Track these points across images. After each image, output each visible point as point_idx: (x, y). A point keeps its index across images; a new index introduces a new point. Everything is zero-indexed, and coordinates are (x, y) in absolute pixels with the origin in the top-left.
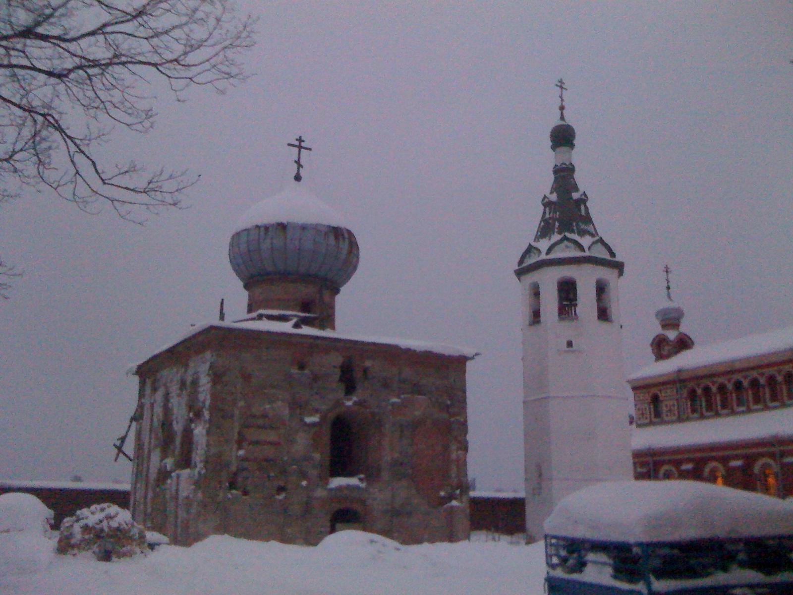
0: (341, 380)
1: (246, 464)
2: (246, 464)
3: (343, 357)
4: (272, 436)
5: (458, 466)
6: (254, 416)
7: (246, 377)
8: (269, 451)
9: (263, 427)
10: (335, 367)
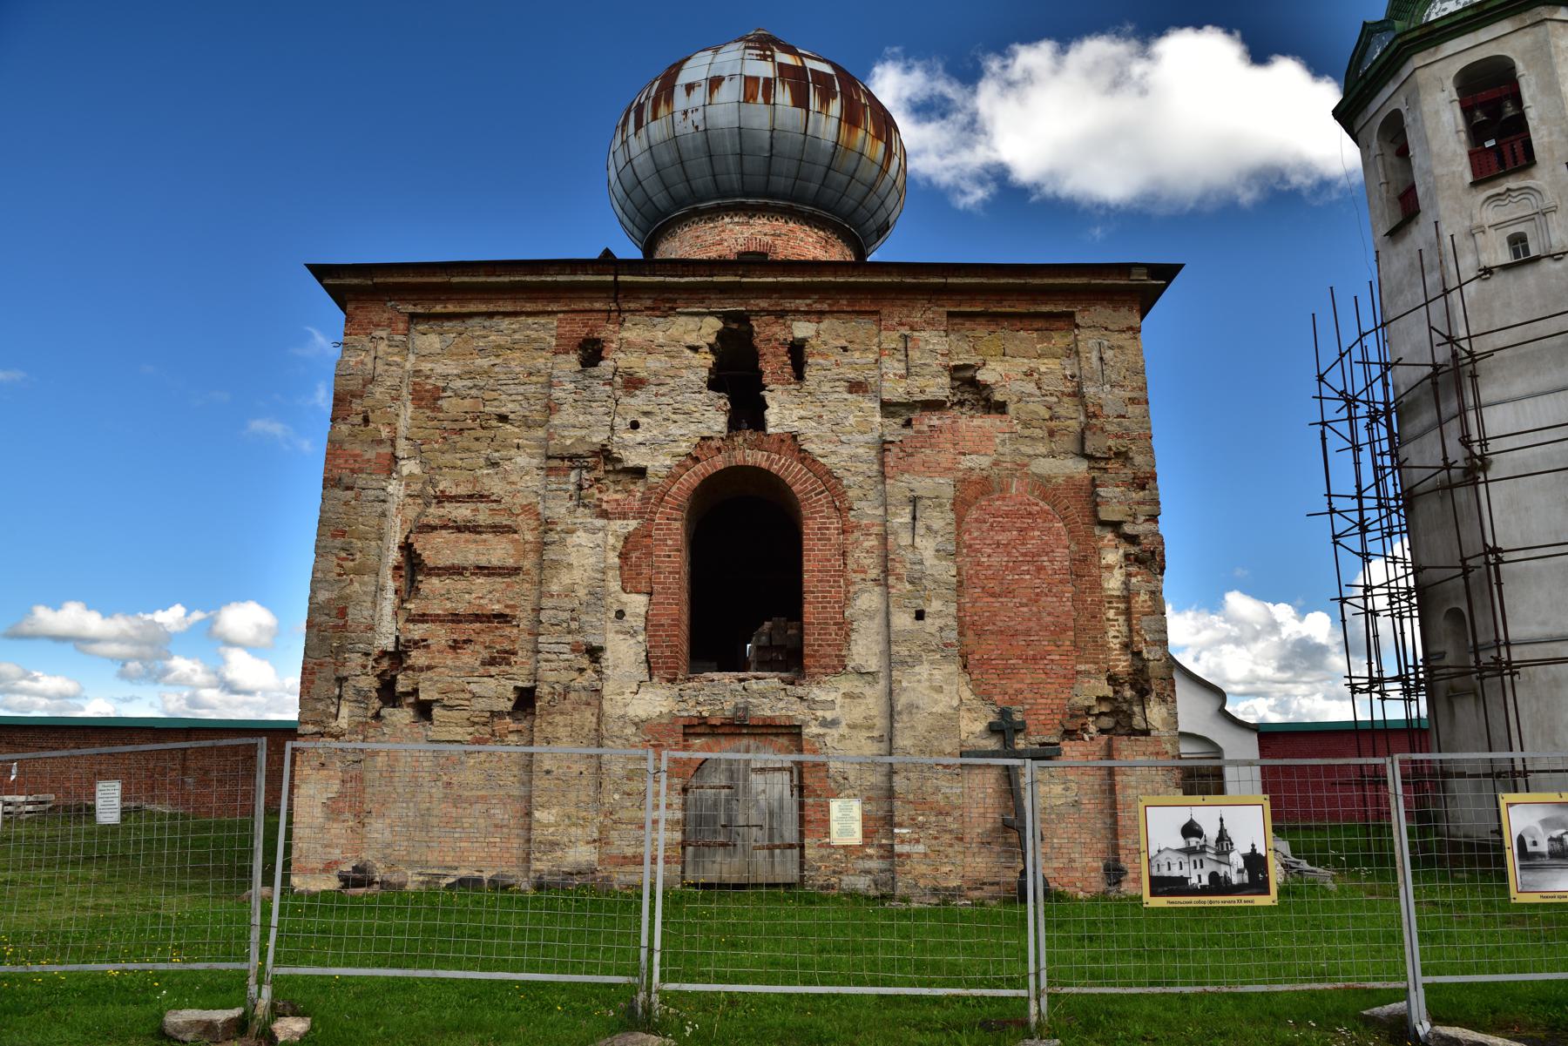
0: (713, 385)
1: (417, 631)
2: (417, 631)
3: (725, 317)
4: (498, 551)
5: (1128, 612)
6: (442, 499)
7: (427, 397)
8: (484, 595)
9: (473, 528)
10: (695, 349)
